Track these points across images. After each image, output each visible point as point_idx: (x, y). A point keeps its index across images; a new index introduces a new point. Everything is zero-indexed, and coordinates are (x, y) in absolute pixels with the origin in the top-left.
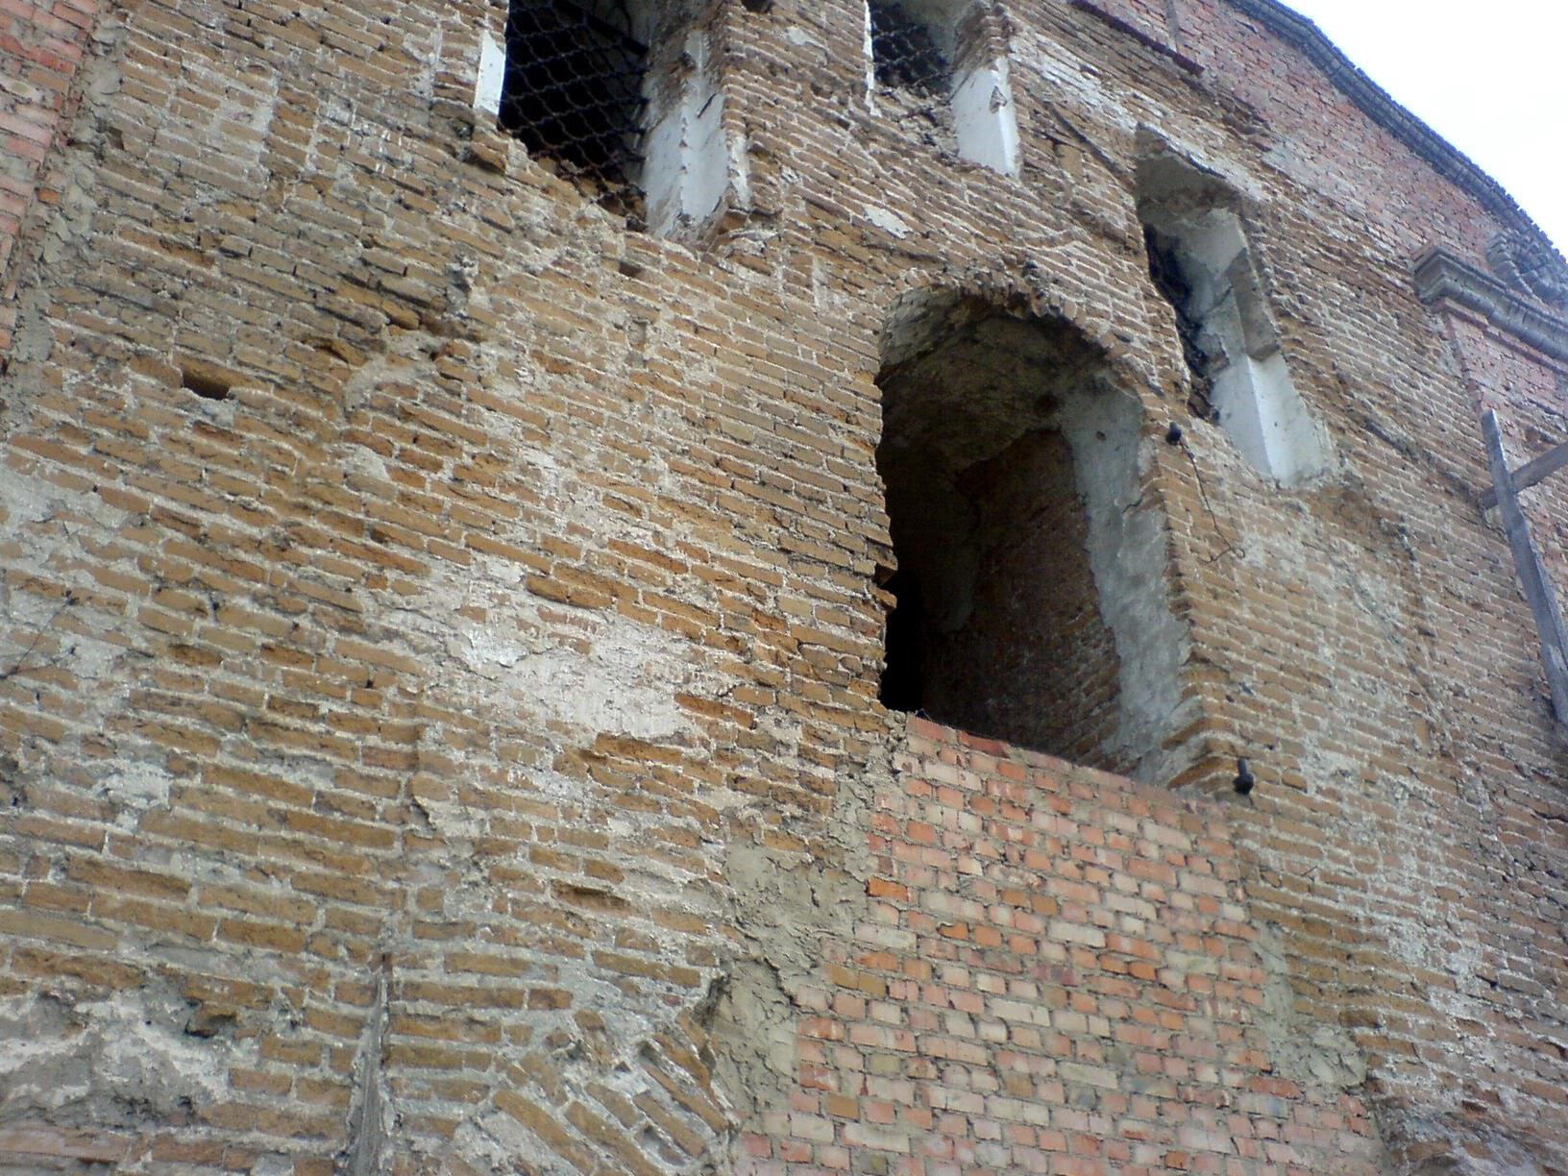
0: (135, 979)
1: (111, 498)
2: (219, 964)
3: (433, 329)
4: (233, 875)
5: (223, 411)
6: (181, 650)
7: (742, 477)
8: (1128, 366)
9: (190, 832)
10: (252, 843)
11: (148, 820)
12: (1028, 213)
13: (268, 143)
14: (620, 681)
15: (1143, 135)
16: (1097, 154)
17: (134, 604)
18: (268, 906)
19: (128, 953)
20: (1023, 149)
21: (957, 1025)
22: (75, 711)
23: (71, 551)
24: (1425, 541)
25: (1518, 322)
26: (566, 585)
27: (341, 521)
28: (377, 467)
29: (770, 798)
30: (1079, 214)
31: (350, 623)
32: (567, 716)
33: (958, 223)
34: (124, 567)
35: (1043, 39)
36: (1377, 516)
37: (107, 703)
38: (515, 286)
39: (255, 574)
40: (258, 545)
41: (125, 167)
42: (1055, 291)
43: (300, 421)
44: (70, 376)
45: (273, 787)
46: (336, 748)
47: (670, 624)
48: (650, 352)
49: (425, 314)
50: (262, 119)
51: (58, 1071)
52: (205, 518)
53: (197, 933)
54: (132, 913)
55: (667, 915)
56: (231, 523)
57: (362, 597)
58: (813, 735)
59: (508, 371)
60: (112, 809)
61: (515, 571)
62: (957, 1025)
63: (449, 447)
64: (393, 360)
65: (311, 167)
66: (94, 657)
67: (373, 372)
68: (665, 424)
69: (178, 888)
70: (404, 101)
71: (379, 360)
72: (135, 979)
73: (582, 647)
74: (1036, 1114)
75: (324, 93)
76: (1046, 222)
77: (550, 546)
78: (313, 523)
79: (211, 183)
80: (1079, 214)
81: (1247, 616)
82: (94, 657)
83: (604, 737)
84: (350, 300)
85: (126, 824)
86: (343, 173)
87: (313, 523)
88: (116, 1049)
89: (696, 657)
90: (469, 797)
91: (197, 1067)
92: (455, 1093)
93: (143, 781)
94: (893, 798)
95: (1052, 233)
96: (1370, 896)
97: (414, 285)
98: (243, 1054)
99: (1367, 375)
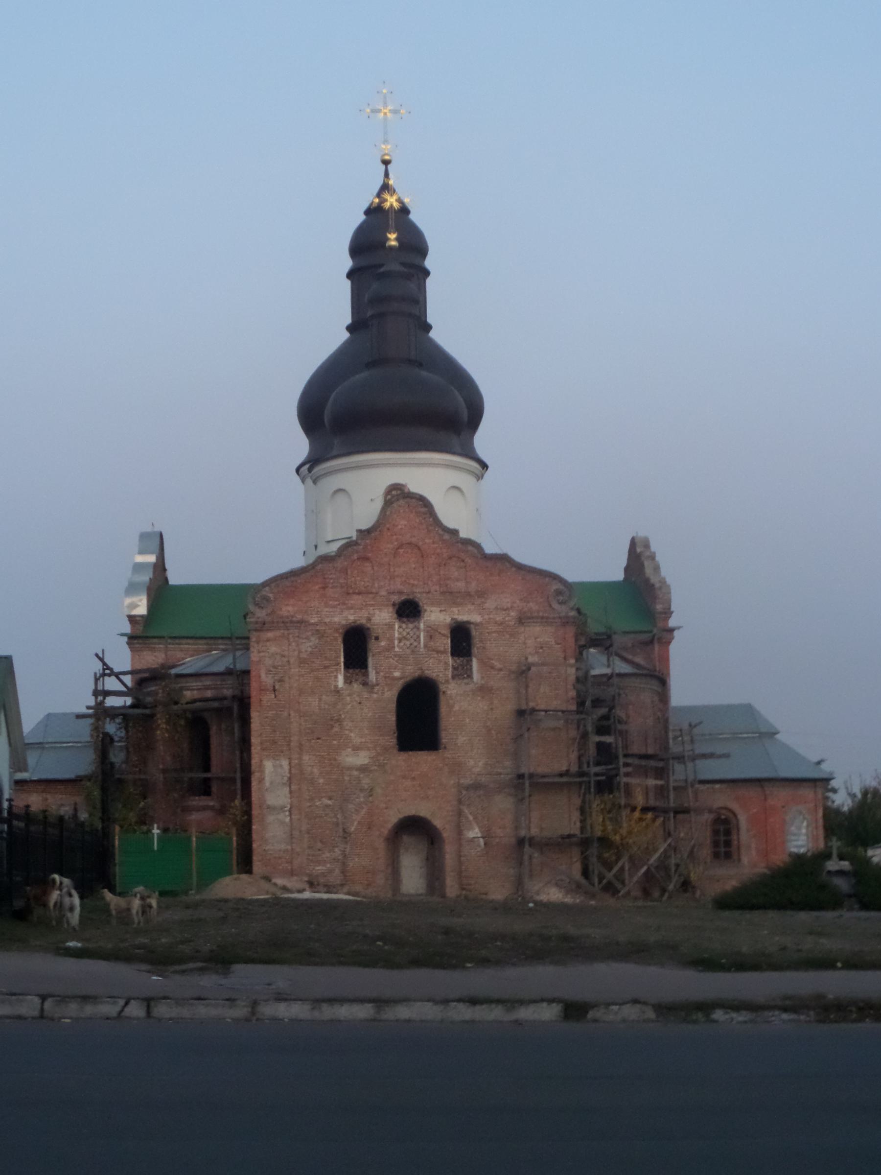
14: (362, 758)
26: (356, 749)
28: (335, 742)
29: (379, 766)
30: (433, 650)
31: (335, 760)
49: (338, 720)
66: (315, 770)
86: (327, 707)
91: (330, 802)
93: (321, 781)
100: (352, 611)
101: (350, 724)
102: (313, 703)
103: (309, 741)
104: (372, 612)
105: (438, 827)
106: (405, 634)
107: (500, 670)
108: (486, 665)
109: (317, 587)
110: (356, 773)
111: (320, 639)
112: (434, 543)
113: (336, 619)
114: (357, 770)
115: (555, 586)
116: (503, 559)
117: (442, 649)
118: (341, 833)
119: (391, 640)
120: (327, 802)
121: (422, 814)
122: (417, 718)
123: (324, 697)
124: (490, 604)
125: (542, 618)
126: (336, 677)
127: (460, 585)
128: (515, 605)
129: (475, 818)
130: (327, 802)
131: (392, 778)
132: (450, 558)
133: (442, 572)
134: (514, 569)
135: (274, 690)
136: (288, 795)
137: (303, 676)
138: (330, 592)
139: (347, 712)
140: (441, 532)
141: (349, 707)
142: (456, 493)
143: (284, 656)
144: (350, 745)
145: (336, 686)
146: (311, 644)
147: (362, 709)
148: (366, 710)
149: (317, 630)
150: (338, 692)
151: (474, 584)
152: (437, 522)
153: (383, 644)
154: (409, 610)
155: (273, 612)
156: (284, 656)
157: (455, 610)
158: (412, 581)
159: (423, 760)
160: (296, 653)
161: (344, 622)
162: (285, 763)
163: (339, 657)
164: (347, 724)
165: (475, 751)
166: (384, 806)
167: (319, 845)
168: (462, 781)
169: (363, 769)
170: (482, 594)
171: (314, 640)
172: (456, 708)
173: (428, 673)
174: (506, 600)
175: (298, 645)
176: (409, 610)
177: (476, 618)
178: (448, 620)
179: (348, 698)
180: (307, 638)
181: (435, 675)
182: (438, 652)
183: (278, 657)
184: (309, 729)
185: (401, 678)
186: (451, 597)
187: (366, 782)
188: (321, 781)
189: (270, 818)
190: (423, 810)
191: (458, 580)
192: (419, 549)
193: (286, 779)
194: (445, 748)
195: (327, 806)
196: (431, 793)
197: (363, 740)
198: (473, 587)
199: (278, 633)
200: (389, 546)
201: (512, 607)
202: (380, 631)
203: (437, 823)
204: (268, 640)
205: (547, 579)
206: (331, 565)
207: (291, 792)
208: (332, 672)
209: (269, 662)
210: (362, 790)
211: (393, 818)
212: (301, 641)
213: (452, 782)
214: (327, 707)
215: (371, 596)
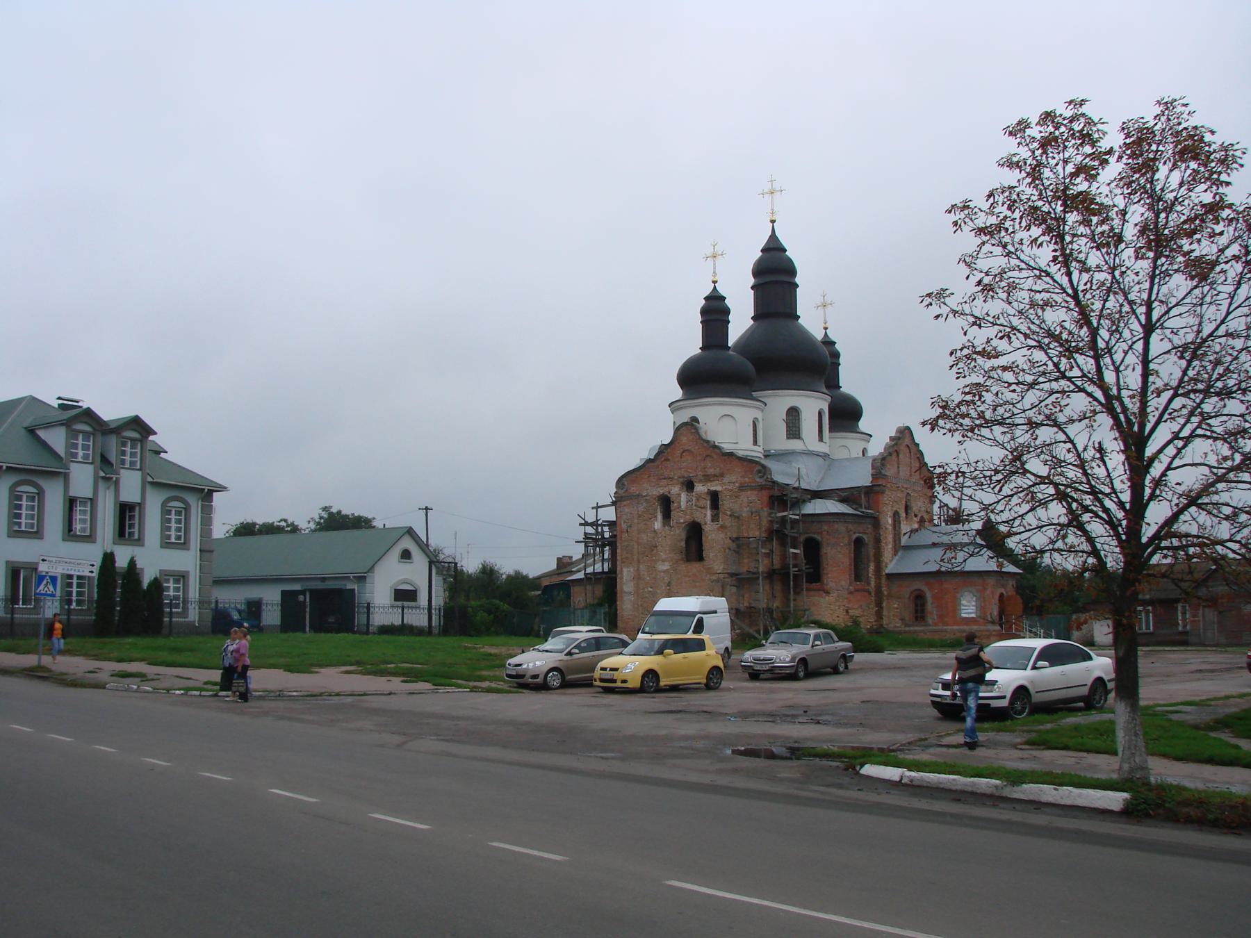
26: (663, 561)
102: (644, 538)
115: (759, 468)
119: (679, 502)
124: (726, 480)
142: (727, 421)
152: (700, 438)
159: (695, 567)
169: (665, 572)
170: (722, 475)
174: (733, 478)
177: (719, 488)
186: (707, 478)
187: (667, 579)
189: (625, 598)
198: (717, 471)
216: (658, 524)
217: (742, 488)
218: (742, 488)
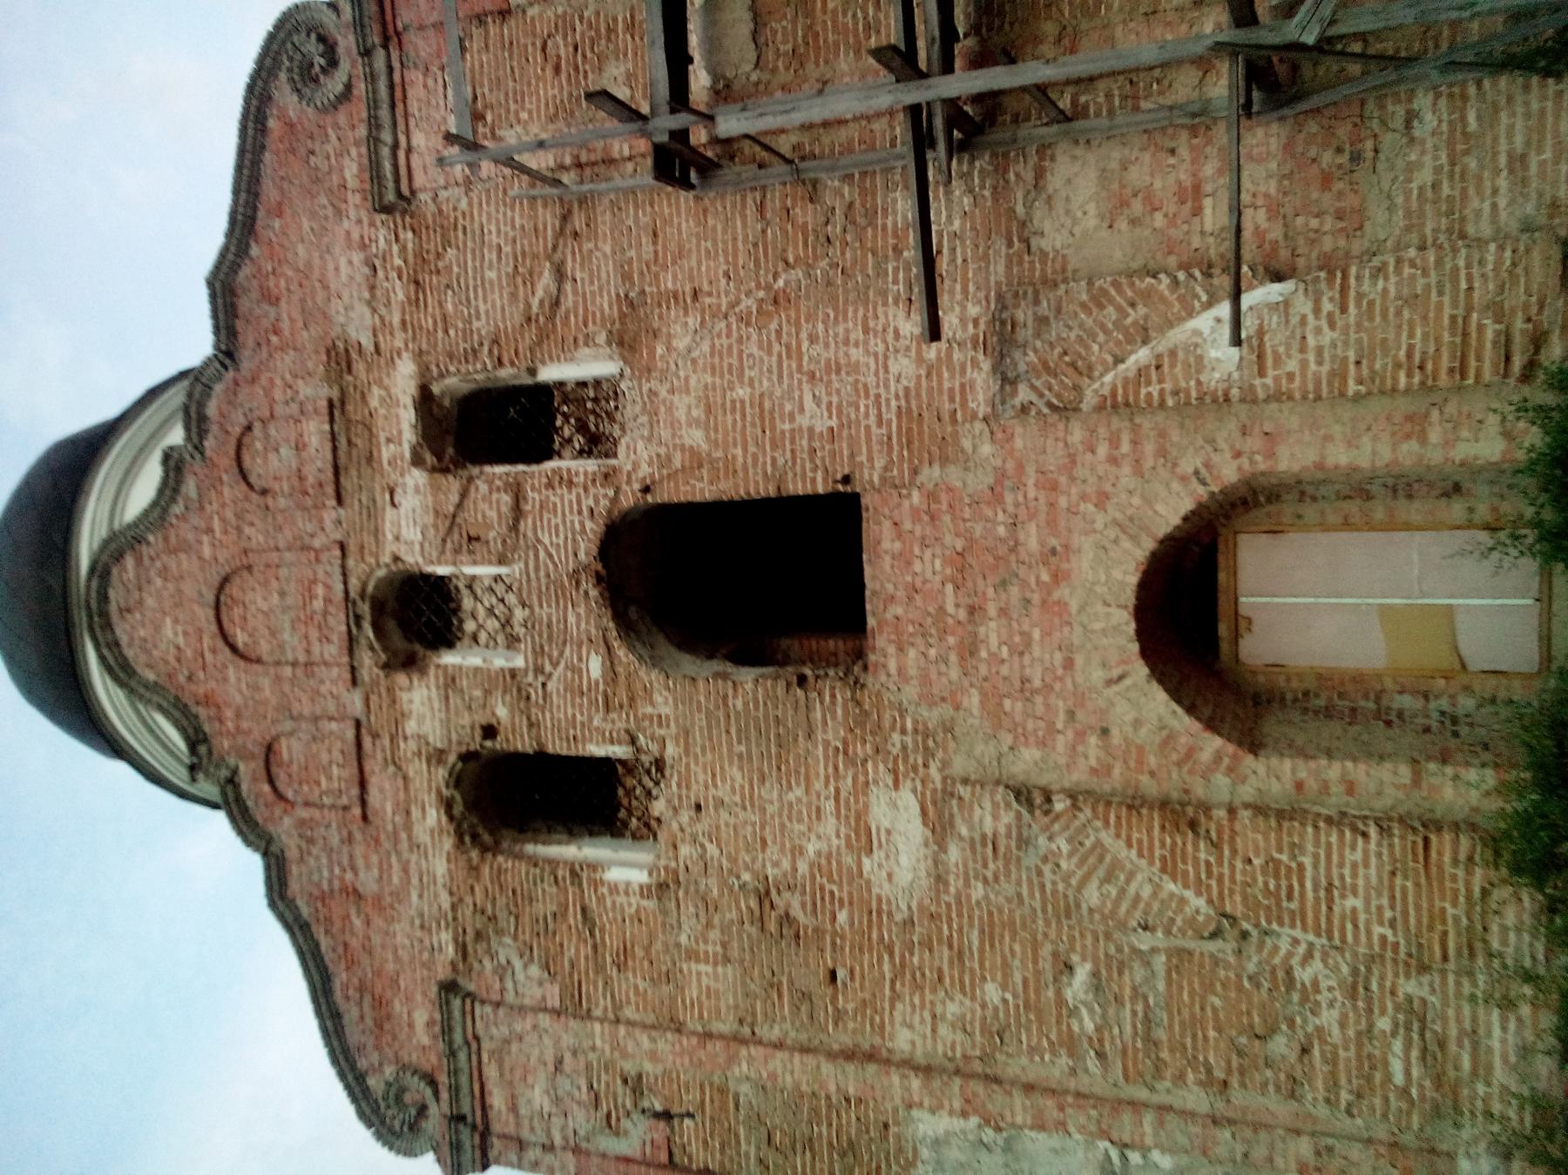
0: (1059, 992)
1: (892, 1007)
2: (1046, 965)
3: (768, 893)
4: (1017, 963)
5: (841, 974)
6: (940, 979)
7: (779, 753)
8: (609, 512)
9: (1005, 976)
10: (1003, 957)
11: (1004, 987)
12: (537, 569)
13: (715, 964)
14: (898, 814)
15: (417, 461)
16: (459, 506)
17: (929, 997)
18: (1024, 953)
19: (1051, 993)
20: (490, 563)
21: (1005, 671)
22: (973, 1012)
23: (917, 1019)
24: (627, 277)
25: (384, 113)
26: (864, 838)
27: (870, 927)
28: (842, 917)
29: (929, 754)
30: (514, 528)
31: (909, 923)
32: (919, 840)
33: (571, 619)
34: (917, 1001)
35: (390, 537)
36: (623, 316)
37: (968, 1002)
38: (733, 860)
39: (903, 957)
40: (891, 955)
41: (754, 1015)
42: (582, 556)
43: (834, 944)
44: (851, 1025)
45: (982, 950)
46: (960, 929)
47: (865, 794)
48: (737, 799)
49: (764, 897)
50: (703, 968)
51: (1091, 1011)
52: (888, 976)
53: (1038, 973)
54: (1037, 993)
55: (995, 817)
56: (886, 967)
57: (898, 917)
58: (893, 728)
59: (776, 864)
60: (1005, 1001)
61: (866, 861)
62: (1005, 671)
63: (822, 889)
64: (788, 905)
65: (719, 948)
66: (952, 1009)
67: (797, 912)
68: (770, 792)
69: (1025, 981)
70: (665, 913)
71: (792, 913)
72: (1059, 992)
73: (888, 832)
74: (1036, 634)
75: (678, 945)
76: (537, 556)
77: (849, 845)
78: (875, 936)
79: (744, 984)
80: (514, 528)
81: (739, 451)
82: (952, 1009)
83: (925, 824)
84: (772, 927)
85: (1009, 996)
86: (714, 935)
87: (875, 936)
88: (1082, 996)
89: (876, 782)
90: (967, 884)
91: (1082, 973)
92: (1078, 906)
94: (911, 692)
95: (542, 554)
96: (882, 391)
97: (753, 903)
98: (1075, 958)
99: (514, 296)
100: (416, 813)
101: (773, 851)
102: (711, 984)
103: (839, 1016)
104: (413, 745)
105: (1187, 505)
106: (492, 624)
107: (560, 274)
108: (548, 327)
109: (357, 922)
110: (954, 854)
111: (500, 933)
112: (209, 531)
113: (440, 867)
114: (943, 848)
116: (225, 289)
117: (506, 499)
118: (1224, 948)
120: (1078, 985)
121: (1127, 576)
122: (754, 581)
123: (683, 939)
125: (374, 124)
126: (614, 889)
127: (315, 431)
128: (356, 236)
129: (1144, 335)
130: (1078, 985)
131: (973, 700)
132: (244, 476)
133: (282, 502)
134: (255, 251)
135: (666, 1116)
136: (1055, 1141)
137: (617, 1007)
138: (367, 881)
139: (733, 860)
140: (178, 509)
141: (712, 849)
143: (559, 1063)
144: (849, 860)
145: (645, 891)
146: (518, 964)
147: (720, 803)
148: (722, 791)
149: (479, 935)
150: (662, 887)
151: (305, 390)
153: (502, 712)
154: (416, 616)
155: (432, 1083)
156: (559, 1063)
157: (386, 452)
158: (318, 604)
160: (545, 1020)
161: (448, 843)
162: (928, 1125)
163: (553, 863)
164: (775, 865)
165: (856, 354)
166: (1093, 740)
167: (1280, 1045)
168: (979, 403)
171: (507, 950)
172: (695, 437)
173: (586, 549)
175: (522, 1010)
176: (416, 616)
177: (404, 379)
178: (417, 477)
179: (685, 850)
180: (503, 971)
181: (589, 525)
182: (518, 511)
183: (564, 1084)
184: (796, 1008)
185: (609, 648)
187: (991, 816)
188: (992, 992)
190: (1108, 577)
191: (300, 447)
192: (225, 580)
193: (989, 1135)
194: (846, 480)
195: (1097, 984)
196: (1032, 538)
197: (829, 806)
199: (491, 1072)
200: (232, 679)
201: (363, 247)
202: (466, 720)
203: (1170, 509)
204: (514, 1109)
205: (272, 123)
206: (294, 869)
207: (1040, 1126)
208: (601, 899)
209: (580, 1120)
210: (1024, 842)
211: (1146, 707)
212: (510, 997)
213: (986, 449)
214: (714, 935)
215: (367, 742)
216: (623, 867)
217: (393, 200)
218: (393, 200)
